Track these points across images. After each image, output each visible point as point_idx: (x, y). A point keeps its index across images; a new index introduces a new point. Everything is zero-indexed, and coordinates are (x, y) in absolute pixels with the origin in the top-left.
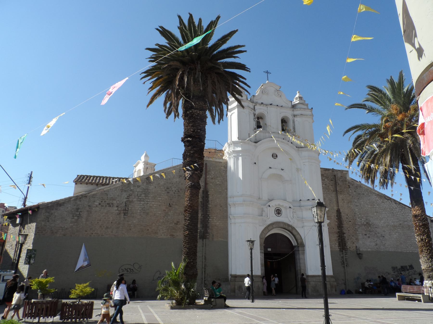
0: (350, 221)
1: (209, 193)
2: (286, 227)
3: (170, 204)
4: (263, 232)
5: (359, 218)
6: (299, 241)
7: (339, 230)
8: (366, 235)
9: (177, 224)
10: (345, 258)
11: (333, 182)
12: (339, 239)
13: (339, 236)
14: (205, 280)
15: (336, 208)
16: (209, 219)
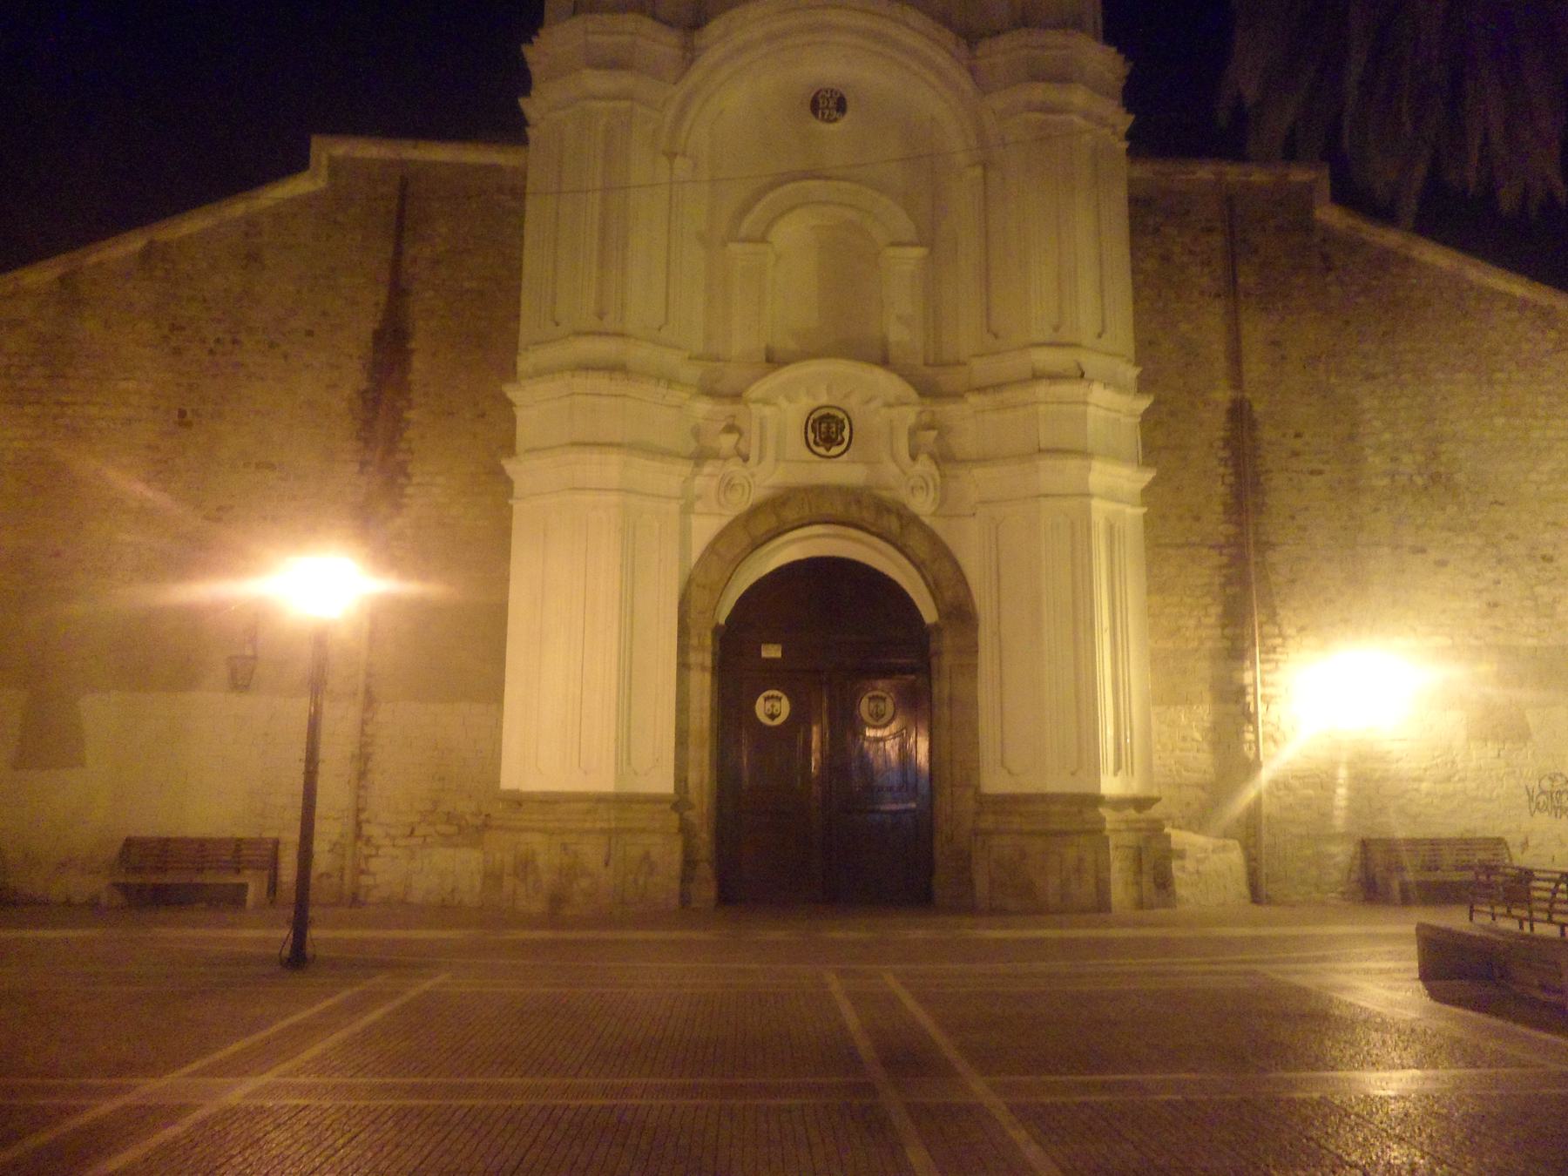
0: (1320, 472)
1: (413, 345)
2: (868, 516)
3: (182, 414)
4: (712, 548)
5: (1379, 448)
6: (949, 595)
7: (1231, 529)
8: (1423, 551)
9: (219, 520)
10: (1260, 691)
11: (1217, 240)
12: (1229, 581)
13: (1229, 566)
14: (359, 825)
15: (1222, 395)
16: (402, 487)
